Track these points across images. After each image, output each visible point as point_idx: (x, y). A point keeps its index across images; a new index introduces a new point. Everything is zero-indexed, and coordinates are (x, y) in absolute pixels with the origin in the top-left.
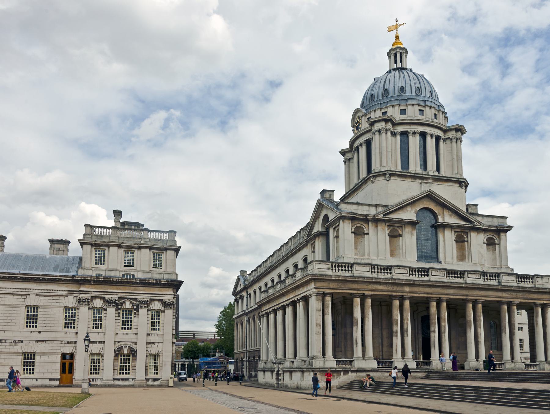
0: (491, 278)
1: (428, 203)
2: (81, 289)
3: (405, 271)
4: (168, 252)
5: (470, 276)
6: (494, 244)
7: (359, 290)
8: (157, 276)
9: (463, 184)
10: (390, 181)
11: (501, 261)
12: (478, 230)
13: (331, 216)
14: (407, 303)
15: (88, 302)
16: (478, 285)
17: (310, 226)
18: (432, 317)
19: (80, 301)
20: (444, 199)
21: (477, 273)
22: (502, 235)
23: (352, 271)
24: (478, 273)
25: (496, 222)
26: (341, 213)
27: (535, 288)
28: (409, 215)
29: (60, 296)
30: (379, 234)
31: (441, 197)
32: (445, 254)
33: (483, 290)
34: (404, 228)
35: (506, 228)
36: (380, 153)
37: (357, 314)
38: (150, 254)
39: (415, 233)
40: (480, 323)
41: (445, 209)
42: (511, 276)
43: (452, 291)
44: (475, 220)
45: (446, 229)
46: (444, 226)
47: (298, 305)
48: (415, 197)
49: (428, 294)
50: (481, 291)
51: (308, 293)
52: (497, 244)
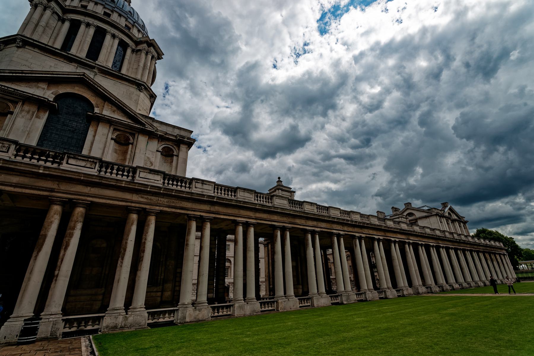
0: (120, 173)
1: (82, 90)
5: (71, 161)
6: (172, 156)
10: (20, 50)
12: (151, 135)
16: (77, 174)
20: (104, 89)
21: (90, 160)
22: (183, 147)
24: (92, 160)
31: (100, 86)
33: (93, 187)
34: (20, 104)
35: (186, 140)
39: (45, 116)
40: (67, 240)
41: (106, 103)
42: (154, 174)
44: (146, 122)
45: (100, 123)
46: (100, 120)
48: (54, 73)
50: (89, 188)
52: (176, 156)
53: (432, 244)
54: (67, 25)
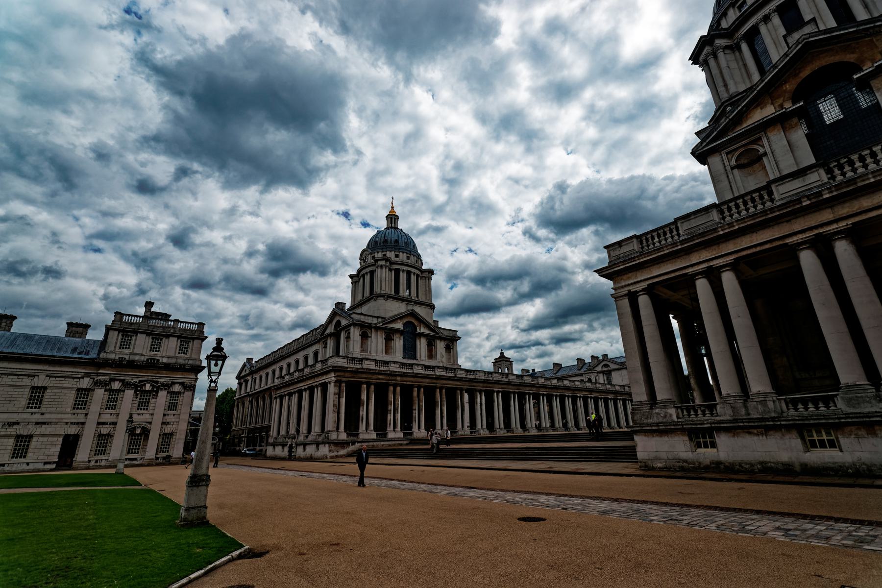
2: (101, 371)
3: (398, 366)
4: (196, 341)
6: (450, 349)
7: (366, 378)
8: (181, 361)
9: (432, 307)
11: (454, 360)
12: (441, 339)
13: (344, 322)
14: (398, 389)
15: (106, 384)
17: (324, 327)
18: (414, 399)
19: (97, 384)
23: (361, 364)
25: (451, 334)
26: (353, 321)
27: (475, 379)
28: (399, 325)
29: (74, 378)
30: (379, 337)
31: (419, 315)
32: (420, 353)
36: (381, 281)
37: (364, 397)
38: (177, 341)
43: (427, 380)
46: (421, 335)
47: (316, 390)
49: (412, 382)
51: (327, 380)
53: (610, 397)
54: (393, 272)
